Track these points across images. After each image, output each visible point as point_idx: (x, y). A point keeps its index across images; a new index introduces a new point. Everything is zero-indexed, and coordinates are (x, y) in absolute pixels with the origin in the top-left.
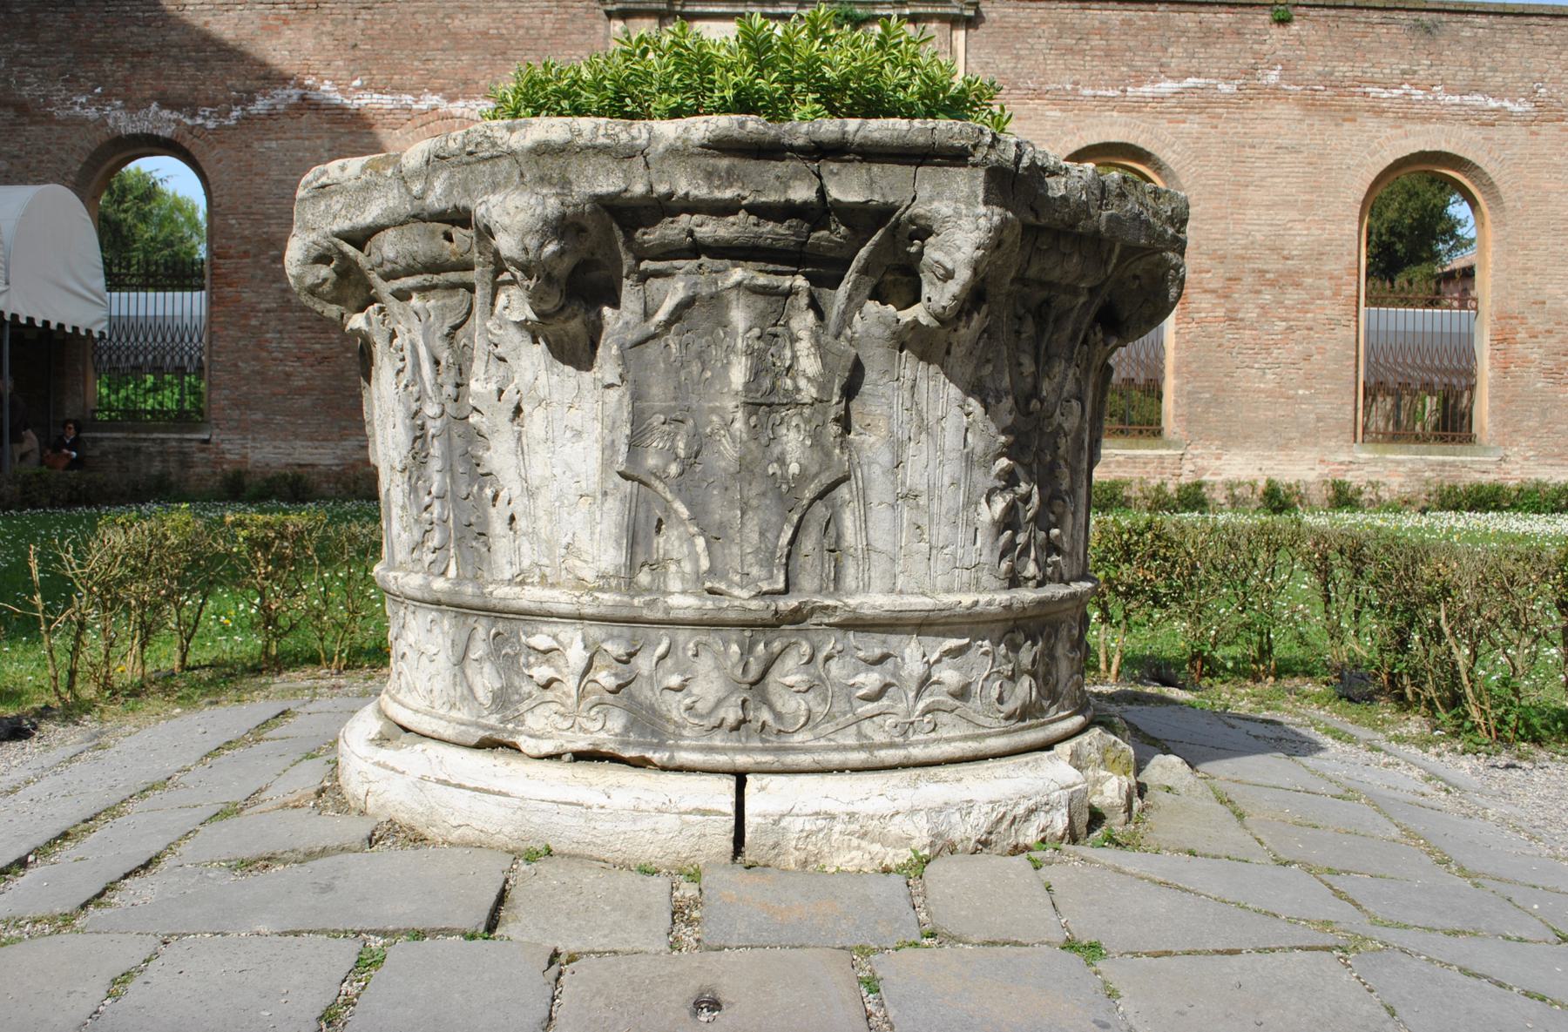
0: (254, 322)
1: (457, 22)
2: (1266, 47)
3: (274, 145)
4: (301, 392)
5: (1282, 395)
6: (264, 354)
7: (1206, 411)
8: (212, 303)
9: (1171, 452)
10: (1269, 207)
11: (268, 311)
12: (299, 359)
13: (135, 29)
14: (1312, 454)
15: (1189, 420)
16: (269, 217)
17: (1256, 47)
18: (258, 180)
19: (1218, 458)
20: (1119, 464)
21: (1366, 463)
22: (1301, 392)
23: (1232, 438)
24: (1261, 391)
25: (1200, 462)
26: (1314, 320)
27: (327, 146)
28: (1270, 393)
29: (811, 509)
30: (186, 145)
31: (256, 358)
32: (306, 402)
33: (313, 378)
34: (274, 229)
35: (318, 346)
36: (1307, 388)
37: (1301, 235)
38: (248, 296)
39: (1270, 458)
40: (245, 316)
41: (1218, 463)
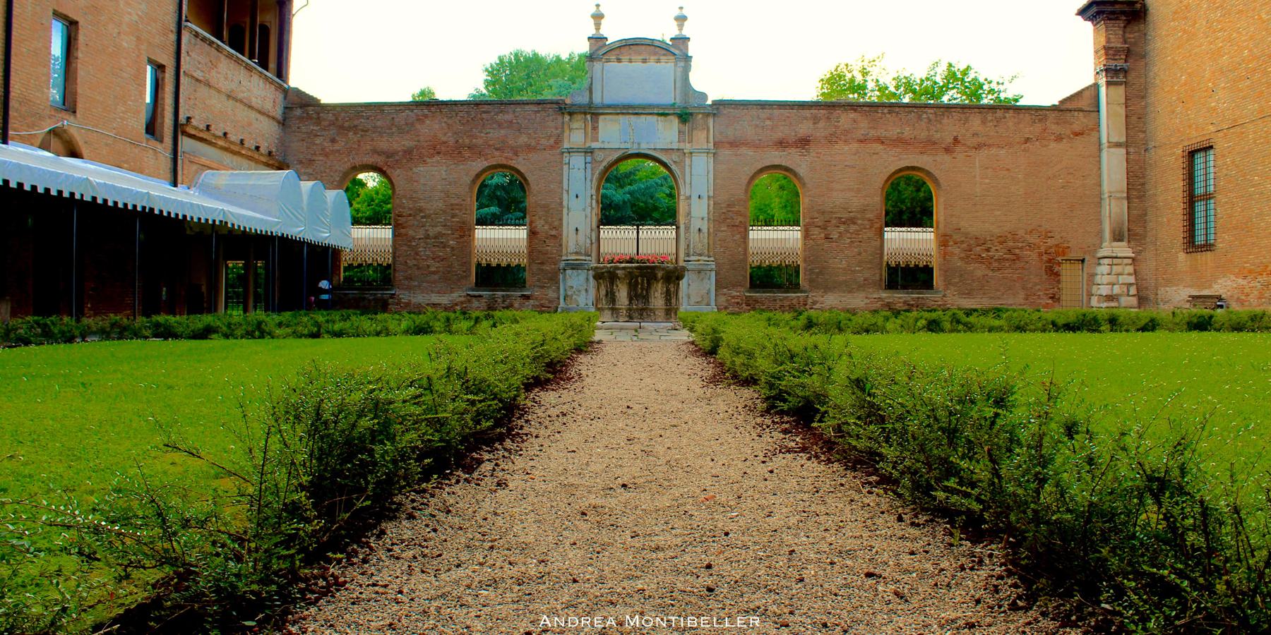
4: (434, 273)
8: (394, 235)
14: (862, 295)
15: (811, 281)
23: (827, 289)
28: (844, 269)
29: (646, 298)
32: (436, 277)
37: (856, 203)
38: (411, 233)
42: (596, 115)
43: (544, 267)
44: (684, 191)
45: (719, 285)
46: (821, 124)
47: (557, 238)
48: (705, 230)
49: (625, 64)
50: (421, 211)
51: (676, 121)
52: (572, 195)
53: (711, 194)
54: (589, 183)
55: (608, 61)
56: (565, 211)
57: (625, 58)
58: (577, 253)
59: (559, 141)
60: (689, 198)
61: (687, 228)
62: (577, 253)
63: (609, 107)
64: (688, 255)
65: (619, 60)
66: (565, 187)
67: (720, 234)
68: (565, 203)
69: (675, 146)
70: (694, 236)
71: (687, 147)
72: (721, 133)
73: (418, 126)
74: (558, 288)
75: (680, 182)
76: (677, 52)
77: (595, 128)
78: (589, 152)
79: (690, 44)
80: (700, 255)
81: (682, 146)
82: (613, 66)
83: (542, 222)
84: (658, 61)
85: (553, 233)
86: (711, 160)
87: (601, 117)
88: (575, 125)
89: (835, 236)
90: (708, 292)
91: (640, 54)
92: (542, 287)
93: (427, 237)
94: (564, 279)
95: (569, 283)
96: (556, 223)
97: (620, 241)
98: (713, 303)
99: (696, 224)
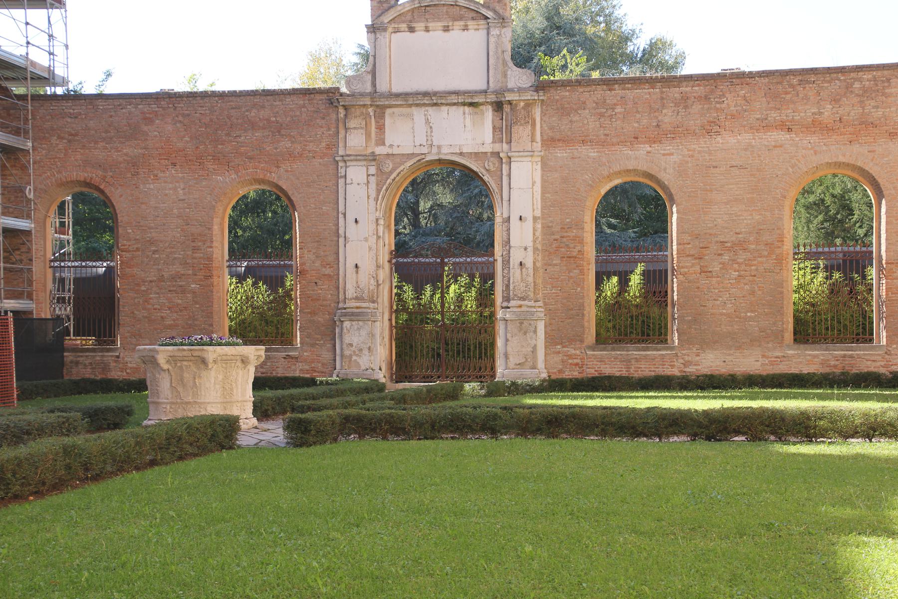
0: (143, 288)
1: (253, 114)
2: (723, 106)
3: (152, 186)
5: (737, 317)
6: (150, 306)
7: (690, 328)
9: (669, 352)
10: (726, 203)
11: (151, 281)
12: (169, 308)
13: (69, 120)
16: (150, 228)
17: (718, 106)
18: (143, 206)
19: (698, 355)
20: (637, 360)
21: (793, 356)
22: (749, 314)
23: (705, 344)
24: (722, 314)
25: (687, 358)
26: (757, 270)
27: (182, 186)
30: (102, 187)
31: (144, 309)
33: (177, 319)
34: (154, 234)
35: (180, 301)
36: (752, 312)
39: (730, 355)
40: (138, 285)
41: (698, 358)
42: (380, 111)
43: (316, 318)
45: (551, 340)
46: (696, 108)
47: (334, 278)
48: (529, 263)
49: (420, 34)
50: (152, 242)
51: (489, 114)
52: (350, 218)
53: (538, 213)
54: (372, 202)
55: (397, 31)
56: (341, 240)
57: (420, 26)
58: (357, 299)
59: (333, 146)
60: (508, 220)
61: (506, 262)
62: (357, 299)
63: (398, 95)
64: (507, 299)
65: (412, 30)
66: (341, 209)
67: (550, 269)
68: (341, 232)
69: (488, 148)
70: (516, 274)
72: (552, 128)
73: (145, 128)
74: (335, 346)
75: (497, 197)
76: (489, 14)
77: (381, 128)
78: (373, 158)
80: (523, 299)
81: (497, 147)
83: (313, 257)
84: (466, 28)
85: (328, 271)
86: (539, 167)
87: (388, 111)
88: (352, 124)
89: (716, 268)
90: (534, 349)
91: (439, 20)
92: (313, 345)
93: (161, 279)
94: (341, 336)
95: (347, 339)
96: (331, 259)
98: (541, 364)
99: (516, 256)
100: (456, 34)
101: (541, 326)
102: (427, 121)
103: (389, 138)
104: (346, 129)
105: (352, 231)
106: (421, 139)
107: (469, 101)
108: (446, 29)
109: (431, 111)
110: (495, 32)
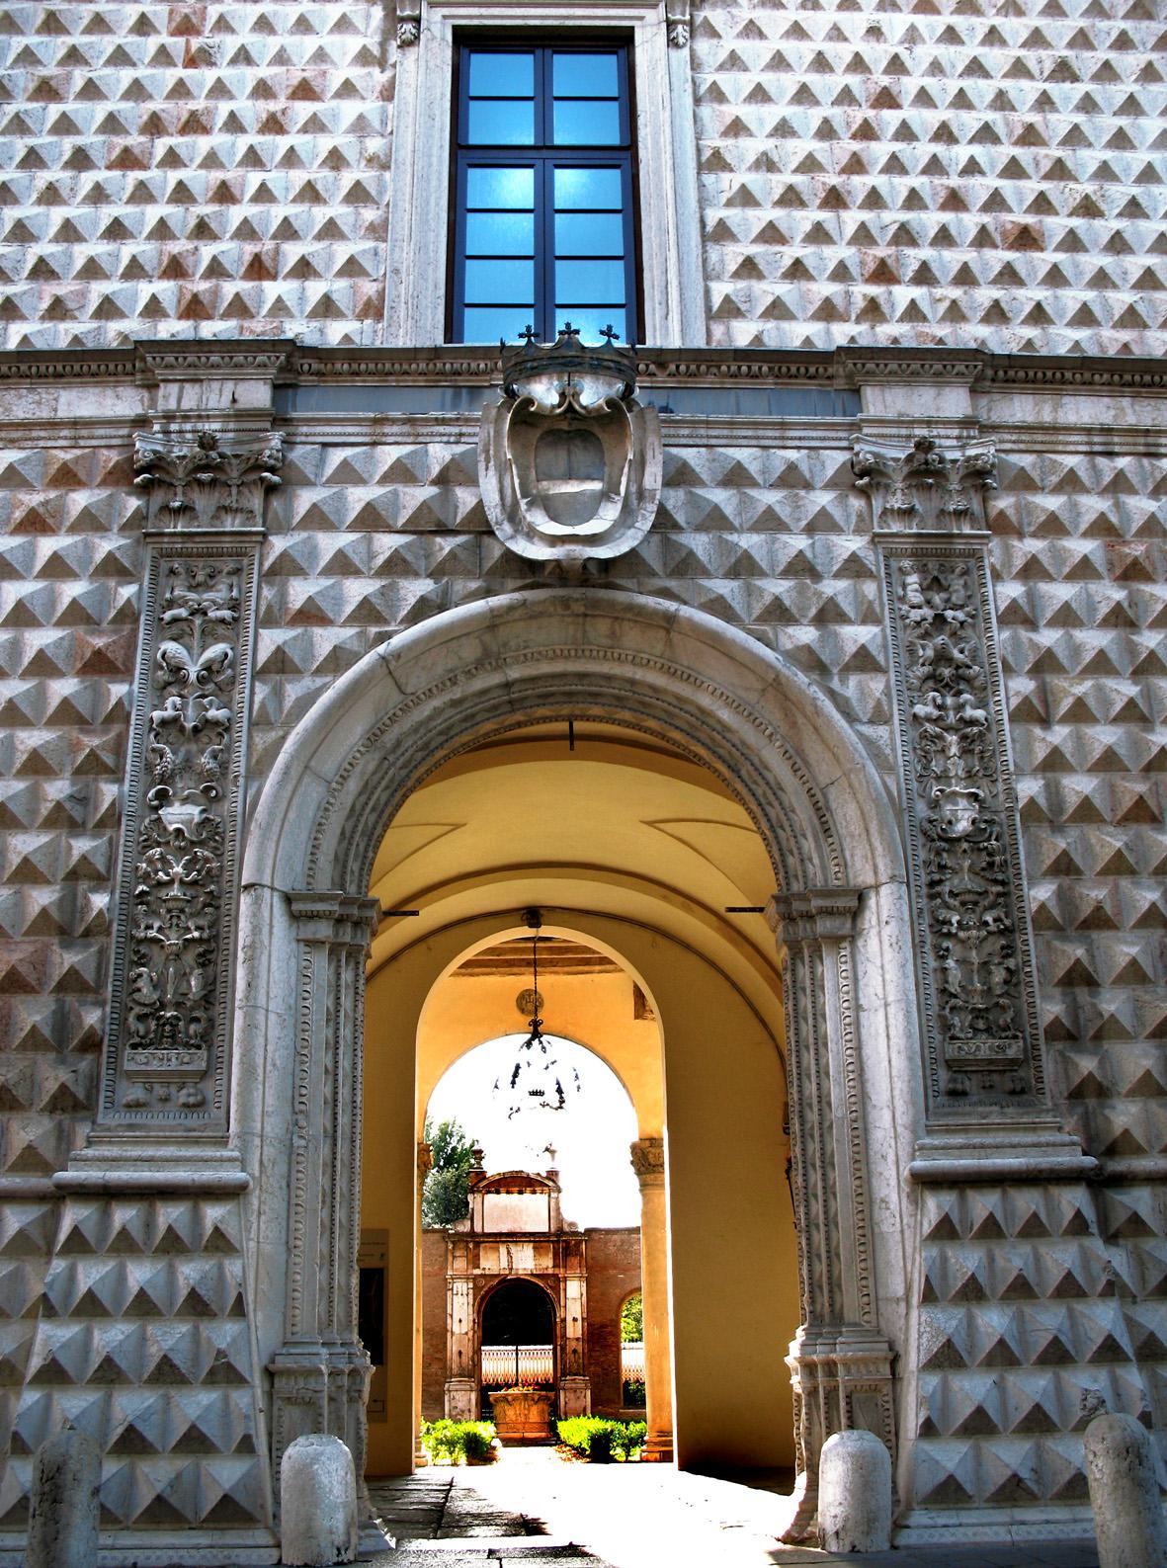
42: (477, 1245)
44: (560, 1314)
52: (456, 1318)
55: (489, 1192)
58: (460, 1376)
60: (564, 1320)
61: (563, 1349)
65: (498, 1192)
69: (550, 1271)
70: (570, 1357)
71: (561, 1272)
77: (477, 1257)
79: (561, 1175)
82: (490, 1198)
84: (534, 1192)
97: (498, 1362)
100: (527, 1196)
101: (589, 1393)
102: (509, 1253)
103: (484, 1263)
104: (454, 1257)
105: (456, 1328)
106: (504, 1263)
107: (536, 1239)
108: (521, 1192)
109: (511, 1246)
110: (553, 1195)
